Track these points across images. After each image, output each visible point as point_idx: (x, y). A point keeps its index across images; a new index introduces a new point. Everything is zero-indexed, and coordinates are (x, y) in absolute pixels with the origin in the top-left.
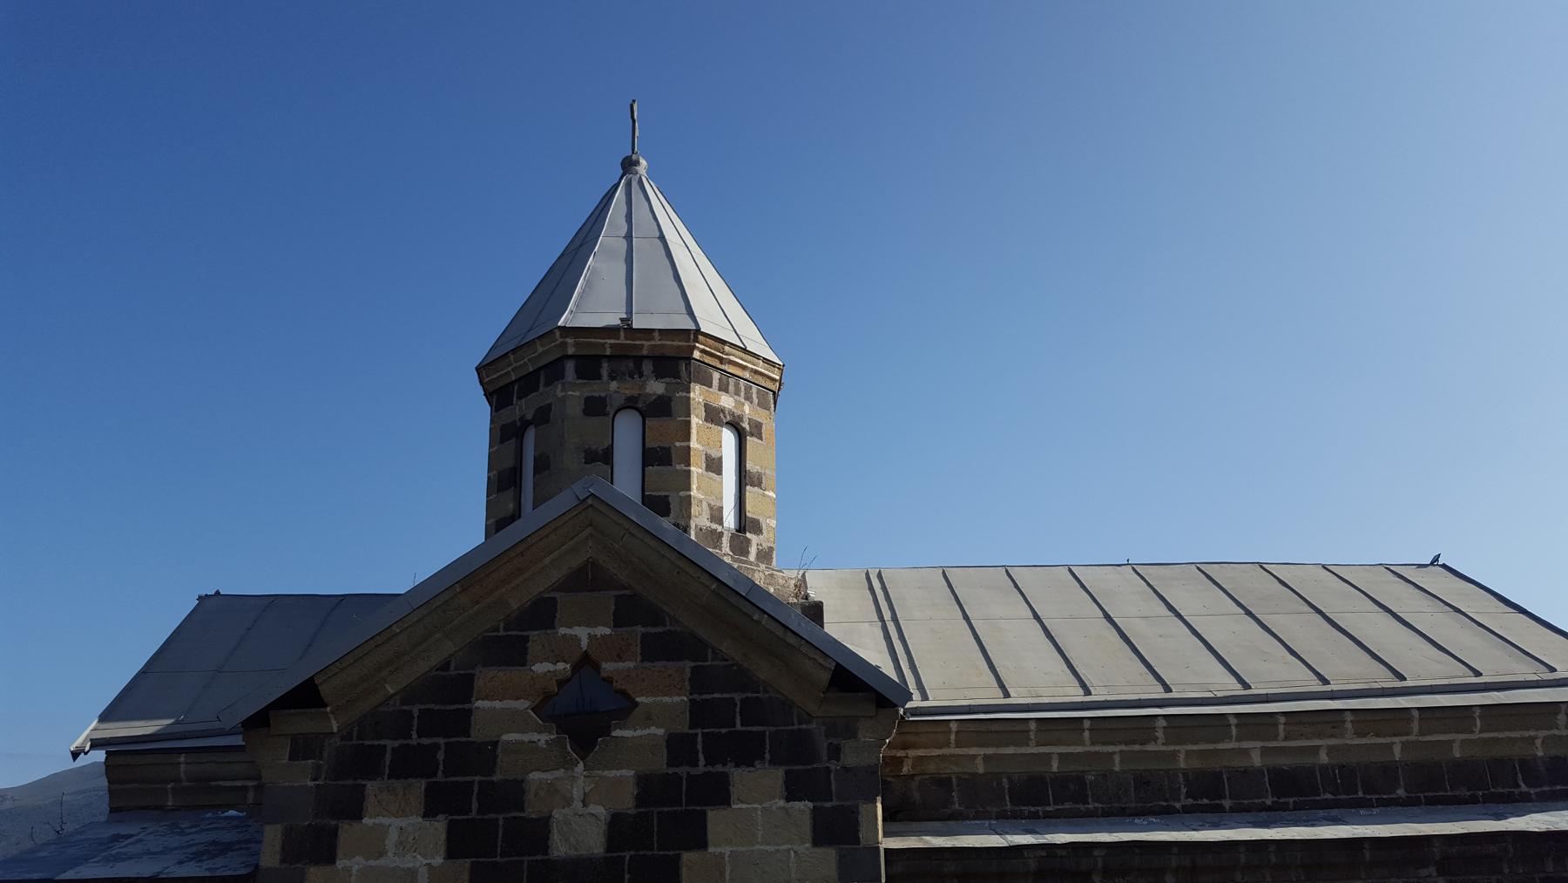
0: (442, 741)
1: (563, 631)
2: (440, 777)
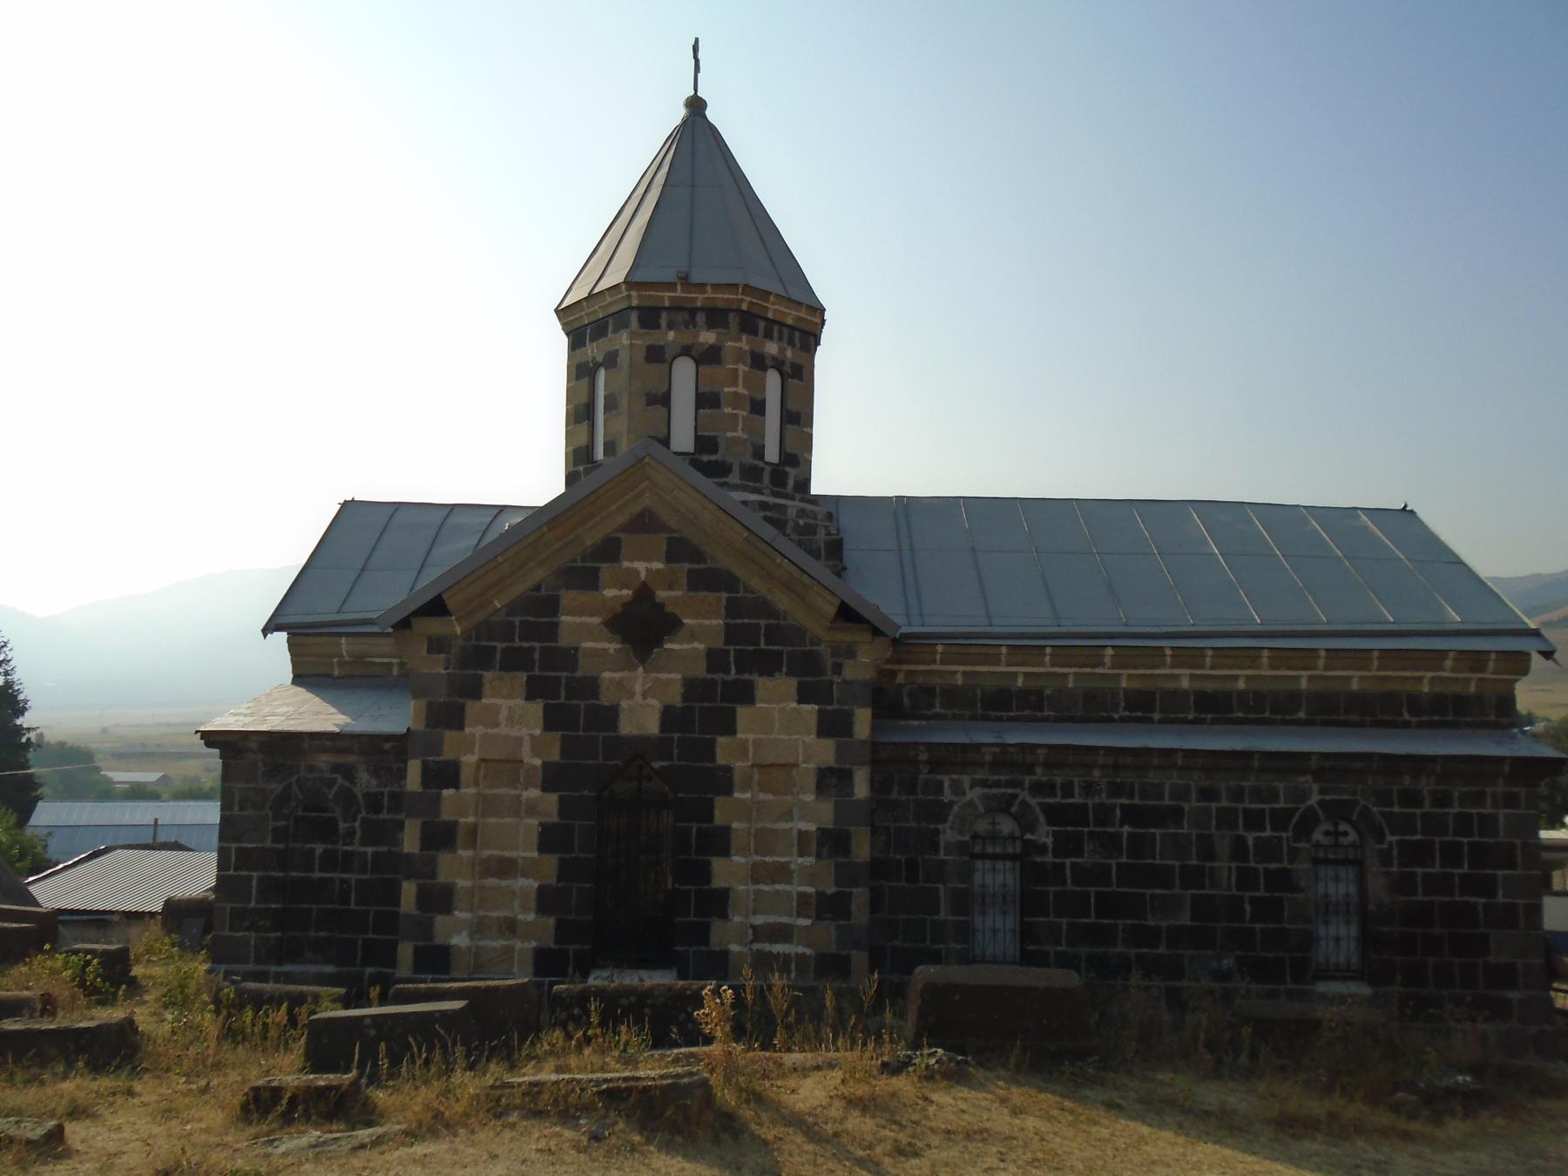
0: (537, 645)
1: (626, 564)
2: (537, 672)
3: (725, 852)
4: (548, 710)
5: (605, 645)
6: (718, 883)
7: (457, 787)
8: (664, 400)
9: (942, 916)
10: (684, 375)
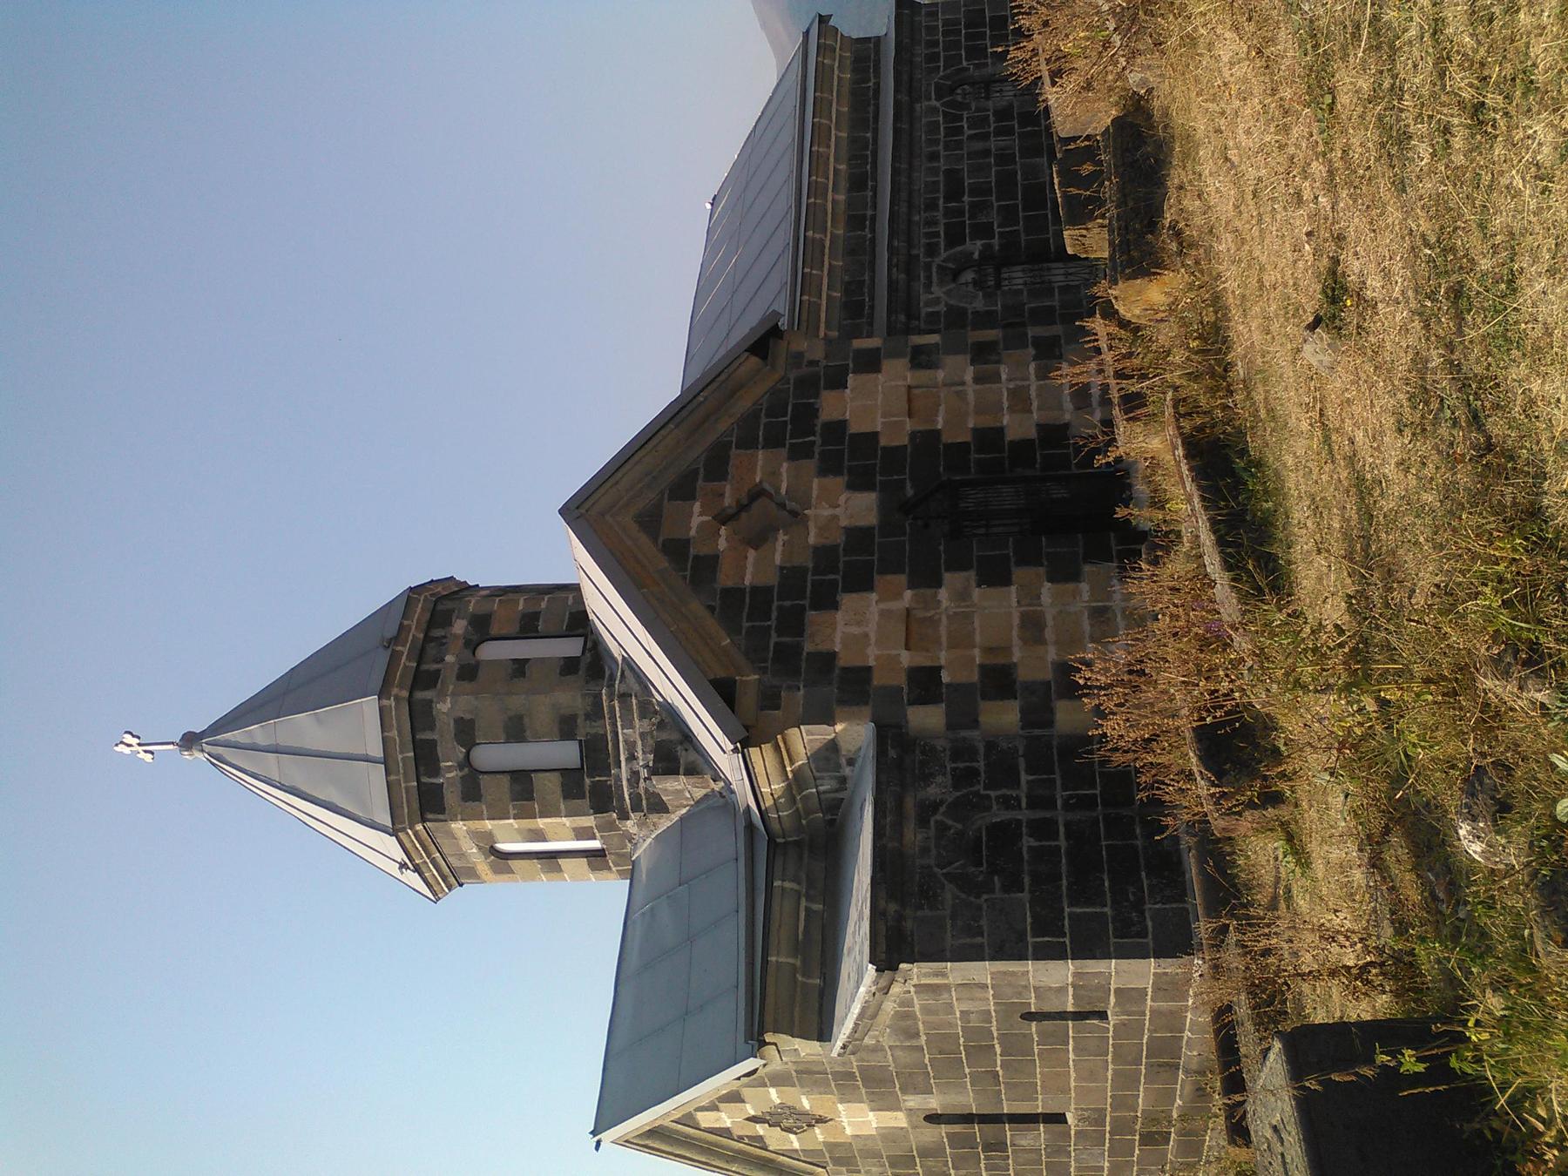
0: (776, 603)
1: (693, 533)
2: (806, 602)
3: (1000, 431)
4: (850, 589)
7: (940, 668)
8: (520, 667)
9: (1056, 303)
10: (492, 651)
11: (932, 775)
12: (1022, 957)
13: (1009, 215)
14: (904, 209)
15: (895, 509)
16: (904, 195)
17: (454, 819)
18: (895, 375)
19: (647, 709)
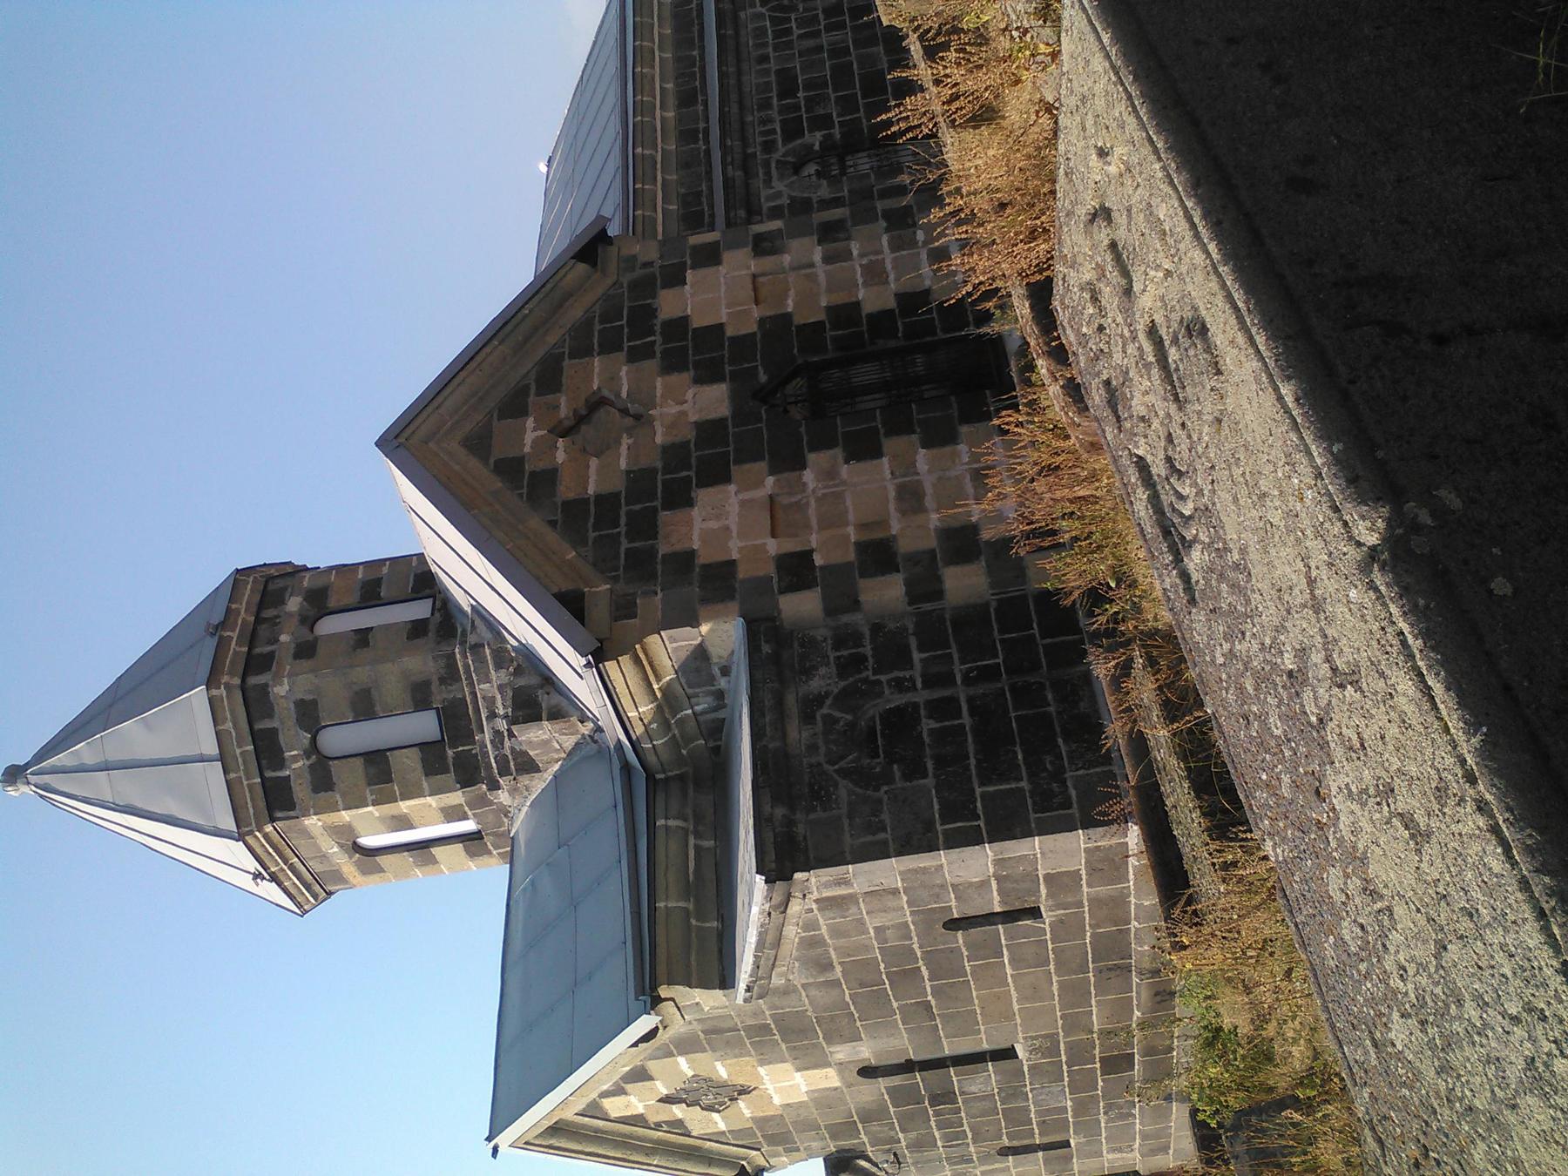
0: (624, 509)
1: (527, 449)
2: (658, 503)
5: (624, 450)
6: (891, 303)
7: (812, 551)
8: (363, 637)
11: (815, 668)
12: (931, 847)
13: (848, 104)
14: (735, 109)
15: (751, 398)
16: (734, 97)
17: (306, 814)
18: (738, 265)
19: (502, 657)
